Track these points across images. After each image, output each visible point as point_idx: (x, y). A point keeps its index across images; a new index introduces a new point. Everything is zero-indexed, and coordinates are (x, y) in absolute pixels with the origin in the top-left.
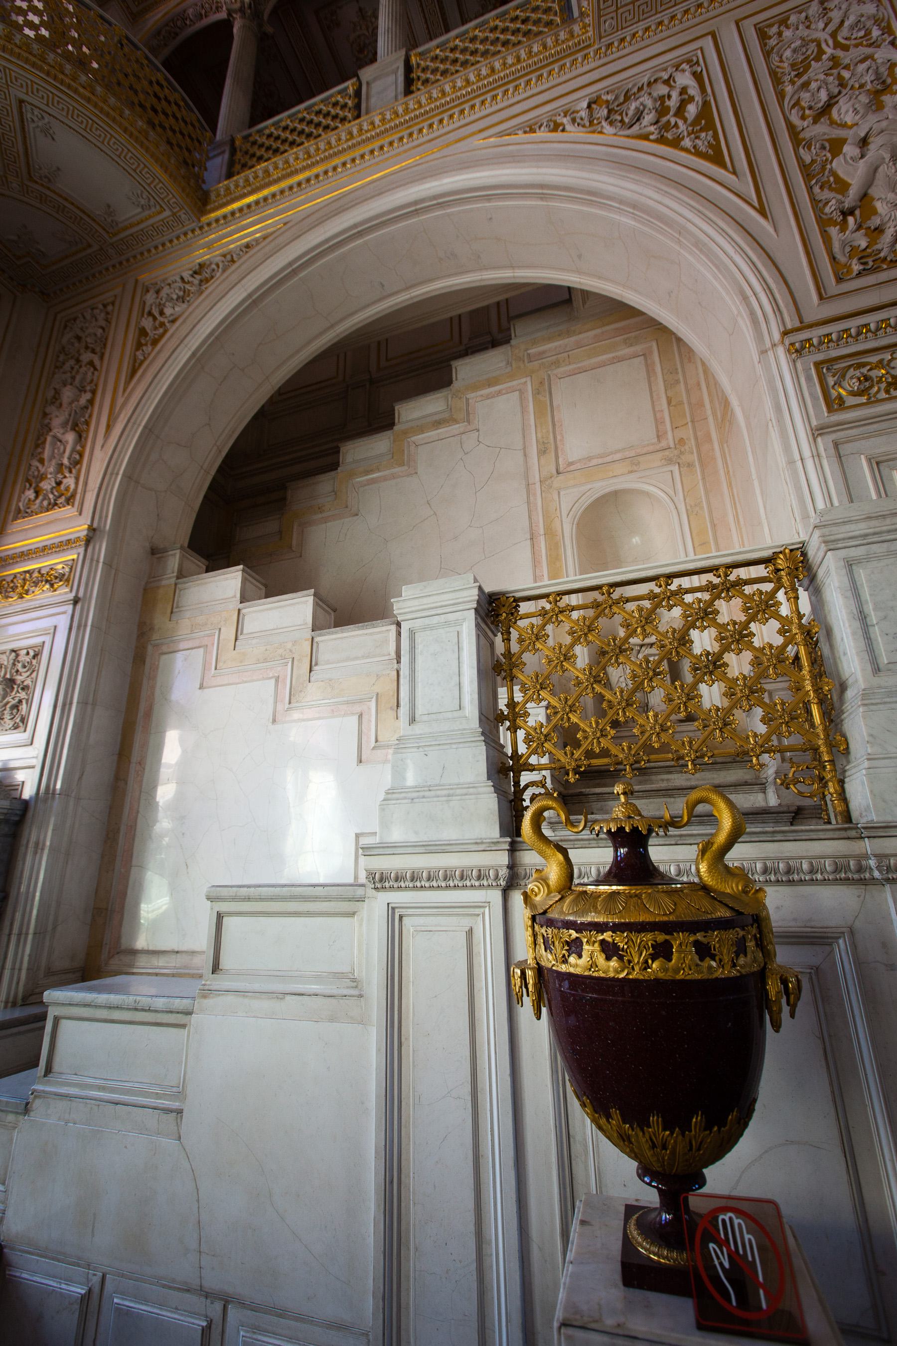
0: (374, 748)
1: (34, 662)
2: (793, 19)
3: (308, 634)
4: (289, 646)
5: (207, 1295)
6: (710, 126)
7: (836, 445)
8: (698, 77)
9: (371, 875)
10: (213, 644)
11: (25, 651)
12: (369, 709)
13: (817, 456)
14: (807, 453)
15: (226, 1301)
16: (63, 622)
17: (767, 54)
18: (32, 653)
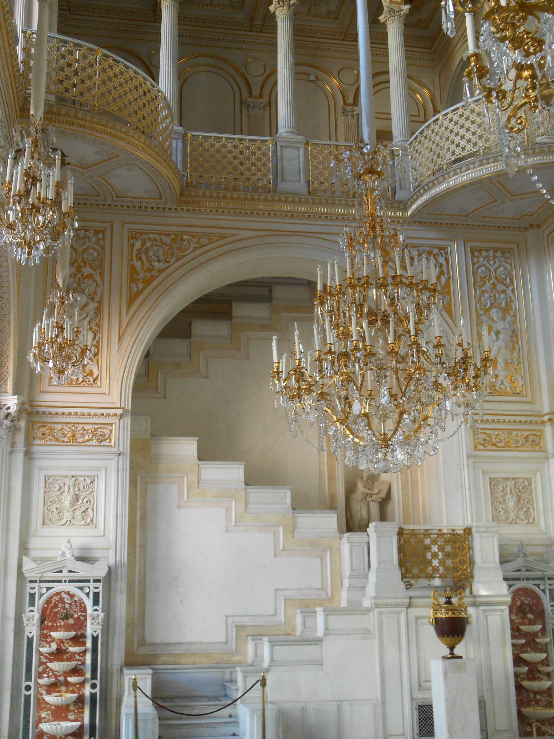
0: (282, 550)
1: (91, 486)
2: (484, 253)
3: (243, 486)
4: (232, 491)
5: (336, 701)
6: (449, 293)
7: (474, 462)
8: (447, 260)
9: (375, 604)
10: (183, 483)
11: (83, 479)
12: (279, 531)
13: (468, 465)
14: (465, 464)
15: (342, 701)
16: (112, 465)
17: (474, 264)
18: (89, 481)
